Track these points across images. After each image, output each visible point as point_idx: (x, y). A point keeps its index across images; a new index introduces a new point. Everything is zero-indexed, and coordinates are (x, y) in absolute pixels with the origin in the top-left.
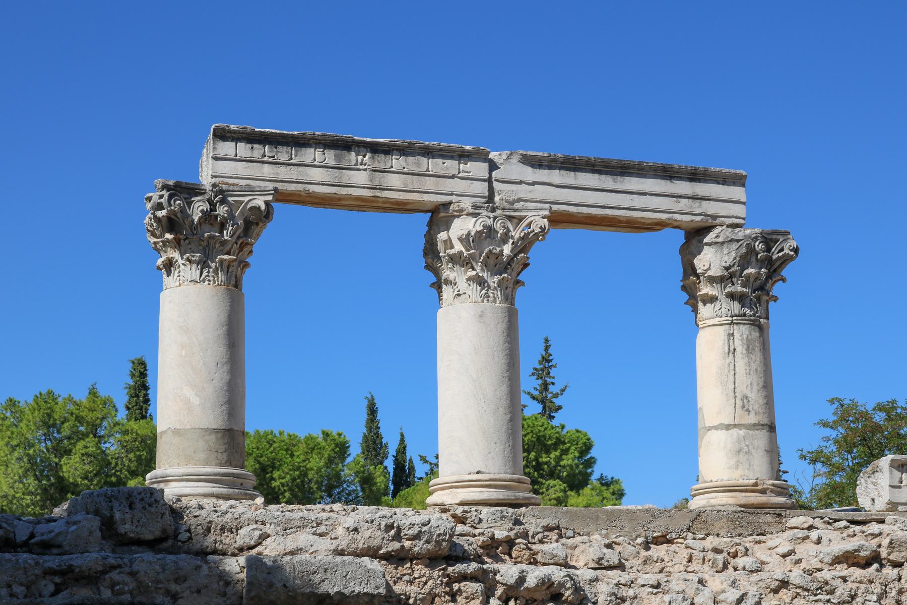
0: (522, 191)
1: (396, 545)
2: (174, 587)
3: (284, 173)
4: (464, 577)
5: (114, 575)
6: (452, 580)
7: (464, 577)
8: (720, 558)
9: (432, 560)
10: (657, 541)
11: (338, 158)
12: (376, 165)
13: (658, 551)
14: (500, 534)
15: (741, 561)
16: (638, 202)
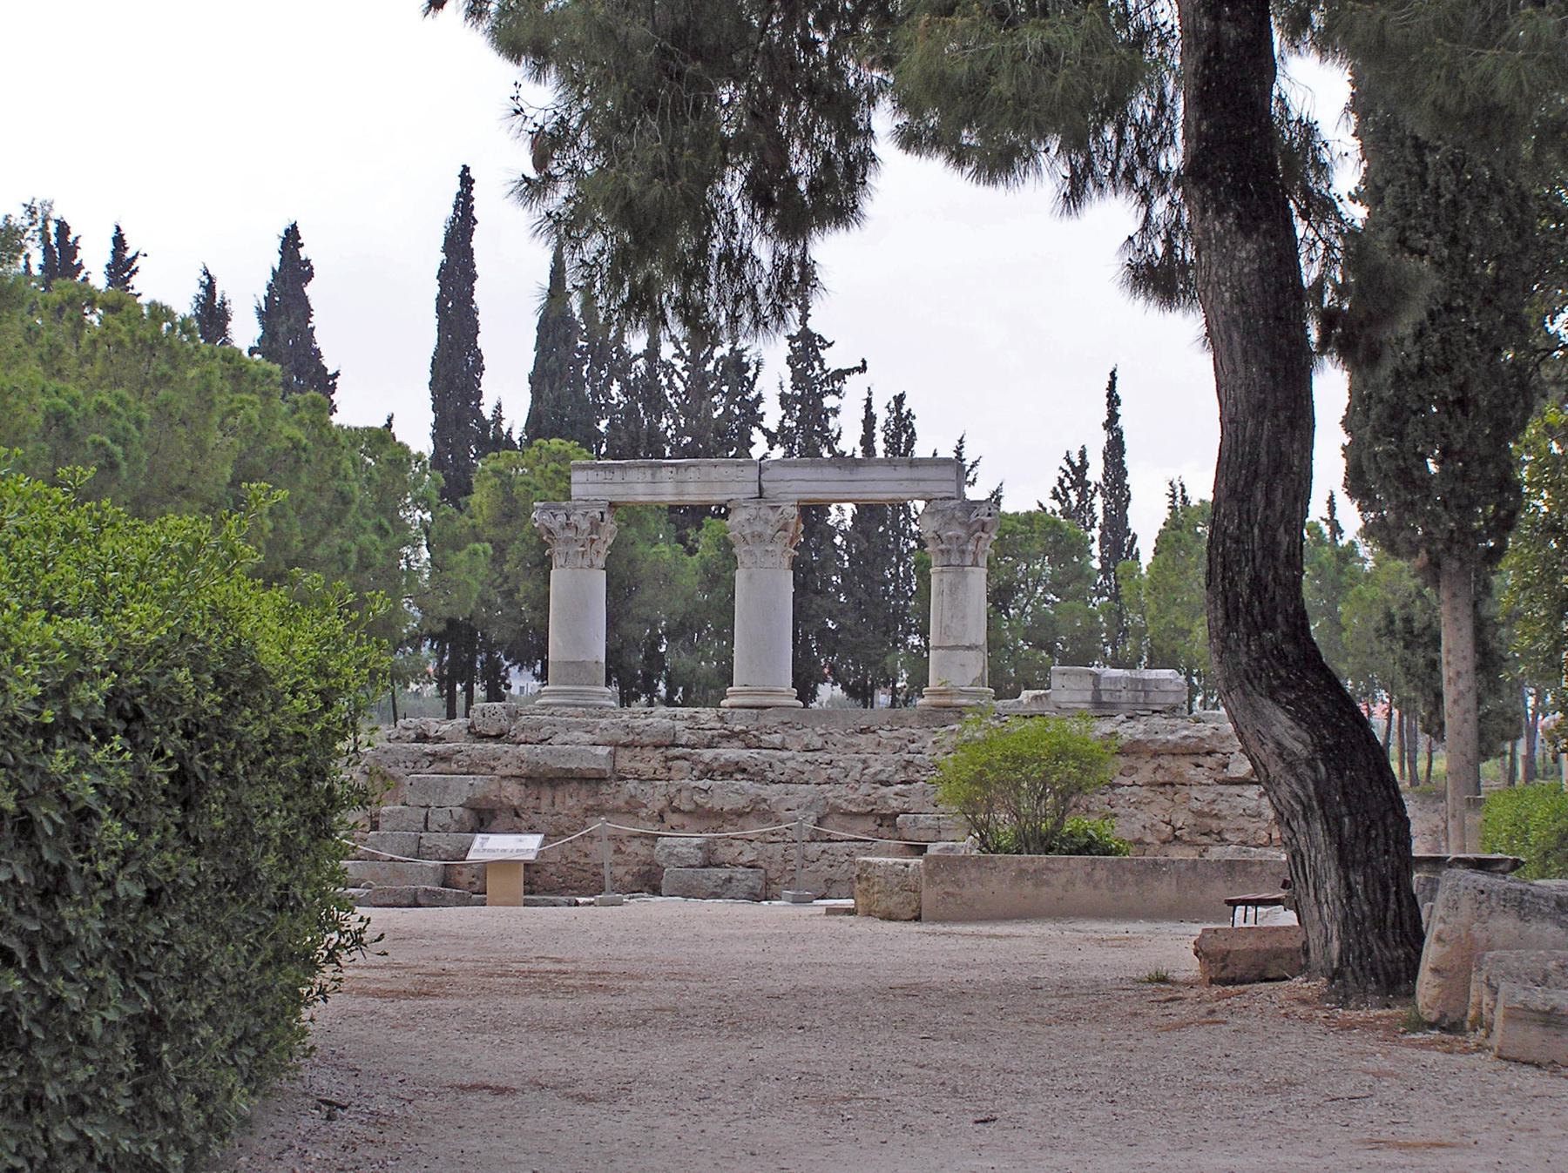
0: (783, 486)
1: (631, 737)
2: (493, 763)
3: (618, 489)
4: (677, 758)
5: (459, 756)
6: (667, 759)
7: (677, 758)
8: (898, 743)
9: (657, 747)
10: (862, 731)
11: (653, 475)
12: (679, 478)
13: (862, 739)
14: (738, 728)
15: (912, 747)
16: (870, 486)
